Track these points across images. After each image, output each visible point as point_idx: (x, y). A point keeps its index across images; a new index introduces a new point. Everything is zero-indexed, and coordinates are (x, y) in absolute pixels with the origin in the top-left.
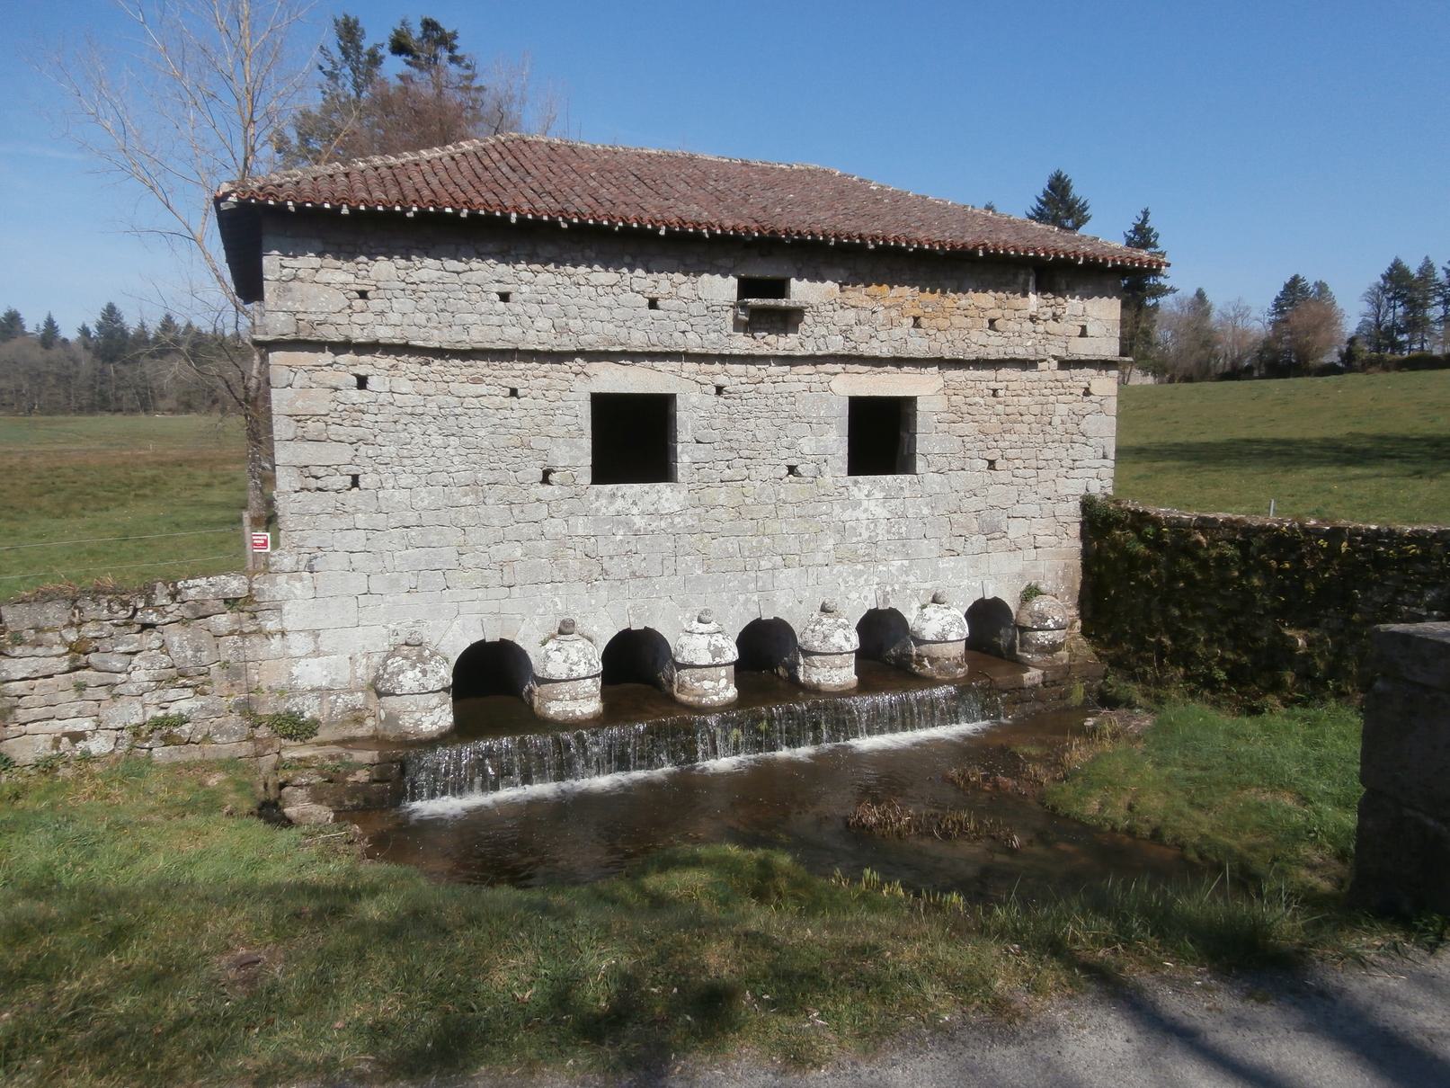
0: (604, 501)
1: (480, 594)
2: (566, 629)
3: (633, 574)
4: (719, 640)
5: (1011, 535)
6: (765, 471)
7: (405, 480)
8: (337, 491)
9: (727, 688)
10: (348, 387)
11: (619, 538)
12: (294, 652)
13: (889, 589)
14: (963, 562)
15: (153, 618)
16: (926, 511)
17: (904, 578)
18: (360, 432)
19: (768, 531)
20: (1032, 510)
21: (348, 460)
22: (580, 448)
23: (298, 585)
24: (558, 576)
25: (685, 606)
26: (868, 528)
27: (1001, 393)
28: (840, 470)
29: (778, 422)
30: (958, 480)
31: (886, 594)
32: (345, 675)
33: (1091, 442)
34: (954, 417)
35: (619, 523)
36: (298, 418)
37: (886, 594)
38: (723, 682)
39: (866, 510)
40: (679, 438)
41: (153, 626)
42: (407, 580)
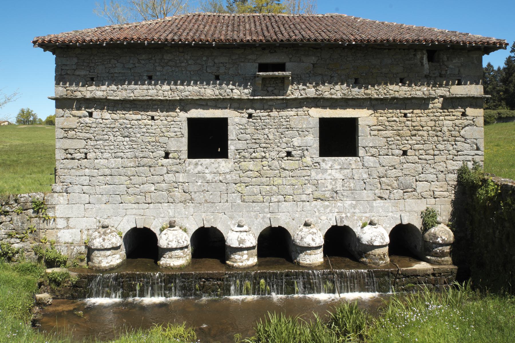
0: (192, 167)
1: (136, 206)
2: (172, 225)
3: (206, 201)
4: (243, 236)
5: (419, 191)
6: (274, 154)
7: (106, 155)
8: (79, 160)
9: (248, 260)
10: (85, 117)
11: (199, 184)
12: (58, 227)
13: (344, 215)
14: (387, 204)
15: (8, 209)
16: (365, 176)
17: (352, 210)
18: (88, 135)
19: (275, 183)
20: (432, 177)
21: (83, 147)
22: (182, 142)
23: (62, 198)
24: (171, 200)
25: (231, 218)
26: (331, 183)
27: (409, 115)
28: (315, 154)
30: (386, 160)
31: (341, 218)
32: (78, 238)
34: (380, 128)
35: (199, 177)
37: (341, 218)
38: (245, 257)
39: (330, 175)
40: (229, 138)
41: (8, 212)
42: (104, 198)
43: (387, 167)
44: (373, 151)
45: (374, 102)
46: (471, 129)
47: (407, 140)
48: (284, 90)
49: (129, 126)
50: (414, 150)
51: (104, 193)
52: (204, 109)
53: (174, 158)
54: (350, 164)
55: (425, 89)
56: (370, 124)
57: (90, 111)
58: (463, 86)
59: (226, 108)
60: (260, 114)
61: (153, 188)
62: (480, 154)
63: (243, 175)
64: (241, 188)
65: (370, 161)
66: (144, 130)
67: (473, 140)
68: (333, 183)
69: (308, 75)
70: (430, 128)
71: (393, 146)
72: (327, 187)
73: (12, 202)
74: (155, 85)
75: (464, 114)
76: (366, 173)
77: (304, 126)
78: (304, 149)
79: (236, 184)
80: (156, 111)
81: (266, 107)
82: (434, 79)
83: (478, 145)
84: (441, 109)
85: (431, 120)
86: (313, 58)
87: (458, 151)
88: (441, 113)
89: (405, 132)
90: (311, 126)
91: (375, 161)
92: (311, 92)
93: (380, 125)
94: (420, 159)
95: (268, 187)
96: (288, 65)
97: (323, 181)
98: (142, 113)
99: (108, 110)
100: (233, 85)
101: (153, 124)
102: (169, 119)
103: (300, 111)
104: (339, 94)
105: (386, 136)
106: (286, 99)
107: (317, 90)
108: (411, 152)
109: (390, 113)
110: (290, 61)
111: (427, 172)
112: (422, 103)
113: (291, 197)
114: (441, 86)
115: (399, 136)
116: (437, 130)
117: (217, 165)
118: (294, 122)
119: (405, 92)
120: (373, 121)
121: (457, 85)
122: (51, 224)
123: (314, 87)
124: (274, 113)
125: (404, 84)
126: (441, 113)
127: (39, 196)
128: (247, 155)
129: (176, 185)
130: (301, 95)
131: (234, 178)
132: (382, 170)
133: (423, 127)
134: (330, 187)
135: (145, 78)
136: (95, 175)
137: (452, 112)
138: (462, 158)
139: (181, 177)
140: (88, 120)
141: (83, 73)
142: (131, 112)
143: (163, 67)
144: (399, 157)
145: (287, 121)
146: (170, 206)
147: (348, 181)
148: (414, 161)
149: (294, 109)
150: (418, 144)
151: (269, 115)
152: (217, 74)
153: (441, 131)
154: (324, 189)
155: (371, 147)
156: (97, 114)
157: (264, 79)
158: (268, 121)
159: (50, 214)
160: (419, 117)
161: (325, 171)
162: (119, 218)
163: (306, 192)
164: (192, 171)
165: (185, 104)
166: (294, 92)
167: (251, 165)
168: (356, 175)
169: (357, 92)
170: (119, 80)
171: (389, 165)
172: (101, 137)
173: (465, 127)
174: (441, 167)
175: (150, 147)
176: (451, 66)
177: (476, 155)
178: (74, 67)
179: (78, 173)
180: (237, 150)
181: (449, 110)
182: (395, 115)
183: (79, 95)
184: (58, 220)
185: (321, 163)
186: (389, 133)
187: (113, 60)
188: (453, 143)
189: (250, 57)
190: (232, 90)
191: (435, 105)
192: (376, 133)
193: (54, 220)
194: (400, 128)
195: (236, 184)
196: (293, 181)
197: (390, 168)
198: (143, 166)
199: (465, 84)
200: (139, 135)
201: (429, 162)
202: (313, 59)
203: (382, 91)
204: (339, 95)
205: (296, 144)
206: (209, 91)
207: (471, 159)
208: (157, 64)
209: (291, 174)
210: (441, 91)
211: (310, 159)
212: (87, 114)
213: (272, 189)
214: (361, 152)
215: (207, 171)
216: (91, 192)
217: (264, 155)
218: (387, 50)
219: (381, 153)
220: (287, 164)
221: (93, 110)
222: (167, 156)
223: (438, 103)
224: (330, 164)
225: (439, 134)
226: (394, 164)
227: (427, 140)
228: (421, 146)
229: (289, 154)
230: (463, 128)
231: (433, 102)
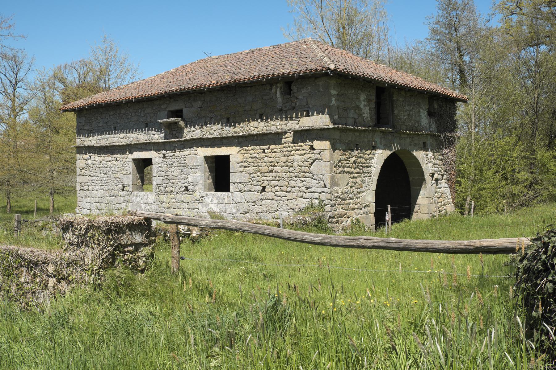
0: (135, 197)
7: (97, 188)
10: (89, 159)
16: (234, 211)
18: (89, 173)
28: (201, 189)
29: (182, 168)
33: (315, 177)
34: (246, 164)
45: (240, 140)
46: (318, 164)
47: (266, 177)
49: (106, 166)
54: (224, 199)
55: (278, 124)
56: (238, 161)
59: (151, 150)
60: (169, 154)
62: (326, 191)
63: (160, 205)
66: (113, 169)
70: (283, 164)
74: (118, 133)
75: (312, 148)
76: (234, 208)
78: (195, 184)
81: (172, 148)
82: (285, 113)
84: (293, 142)
85: (284, 156)
87: (307, 188)
89: (264, 169)
90: (198, 164)
93: (245, 162)
94: (276, 195)
96: (185, 111)
98: (112, 156)
100: (155, 131)
105: (249, 172)
108: (268, 188)
110: (186, 107)
111: (281, 209)
114: (291, 119)
116: (289, 165)
117: (146, 197)
119: (262, 128)
120: (240, 158)
121: (306, 116)
123: (200, 128)
124: (177, 154)
128: (163, 189)
133: (278, 163)
135: (113, 129)
137: (302, 146)
138: (310, 195)
140: (89, 162)
141: (87, 127)
149: (189, 149)
150: (274, 180)
153: (292, 167)
156: (93, 156)
158: (173, 160)
160: (275, 152)
167: (164, 198)
168: (228, 210)
169: (228, 131)
170: (101, 132)
172: (94, 174)
176: (300, 97)
177: (323, 192)
178: (84, 124)
181: (300, 144)
183: (86, 144)
186: (251, 169)
188: (303, 179)
189: (162, 107)
190: (154, 135)
194: (260, 164)
197: (253, 204)
198: (113, 196)
199: (312, 115)
202: (199, 103)
204: (216, 135)
210: (293, 125)
214: (232, 187)
215: (142, 202)
217: (171, 189)
218: (249, 88)
219: (246, 189)
220: (186, 197)
221: (91, 154)
222: (123, 190)
223: (289, 137)
224: (211, 198)
225: (291, 169)
226: (255, 200)
227: (280, 176)
229: (187, 189)
230: (312, 163)
231: (285, 136)
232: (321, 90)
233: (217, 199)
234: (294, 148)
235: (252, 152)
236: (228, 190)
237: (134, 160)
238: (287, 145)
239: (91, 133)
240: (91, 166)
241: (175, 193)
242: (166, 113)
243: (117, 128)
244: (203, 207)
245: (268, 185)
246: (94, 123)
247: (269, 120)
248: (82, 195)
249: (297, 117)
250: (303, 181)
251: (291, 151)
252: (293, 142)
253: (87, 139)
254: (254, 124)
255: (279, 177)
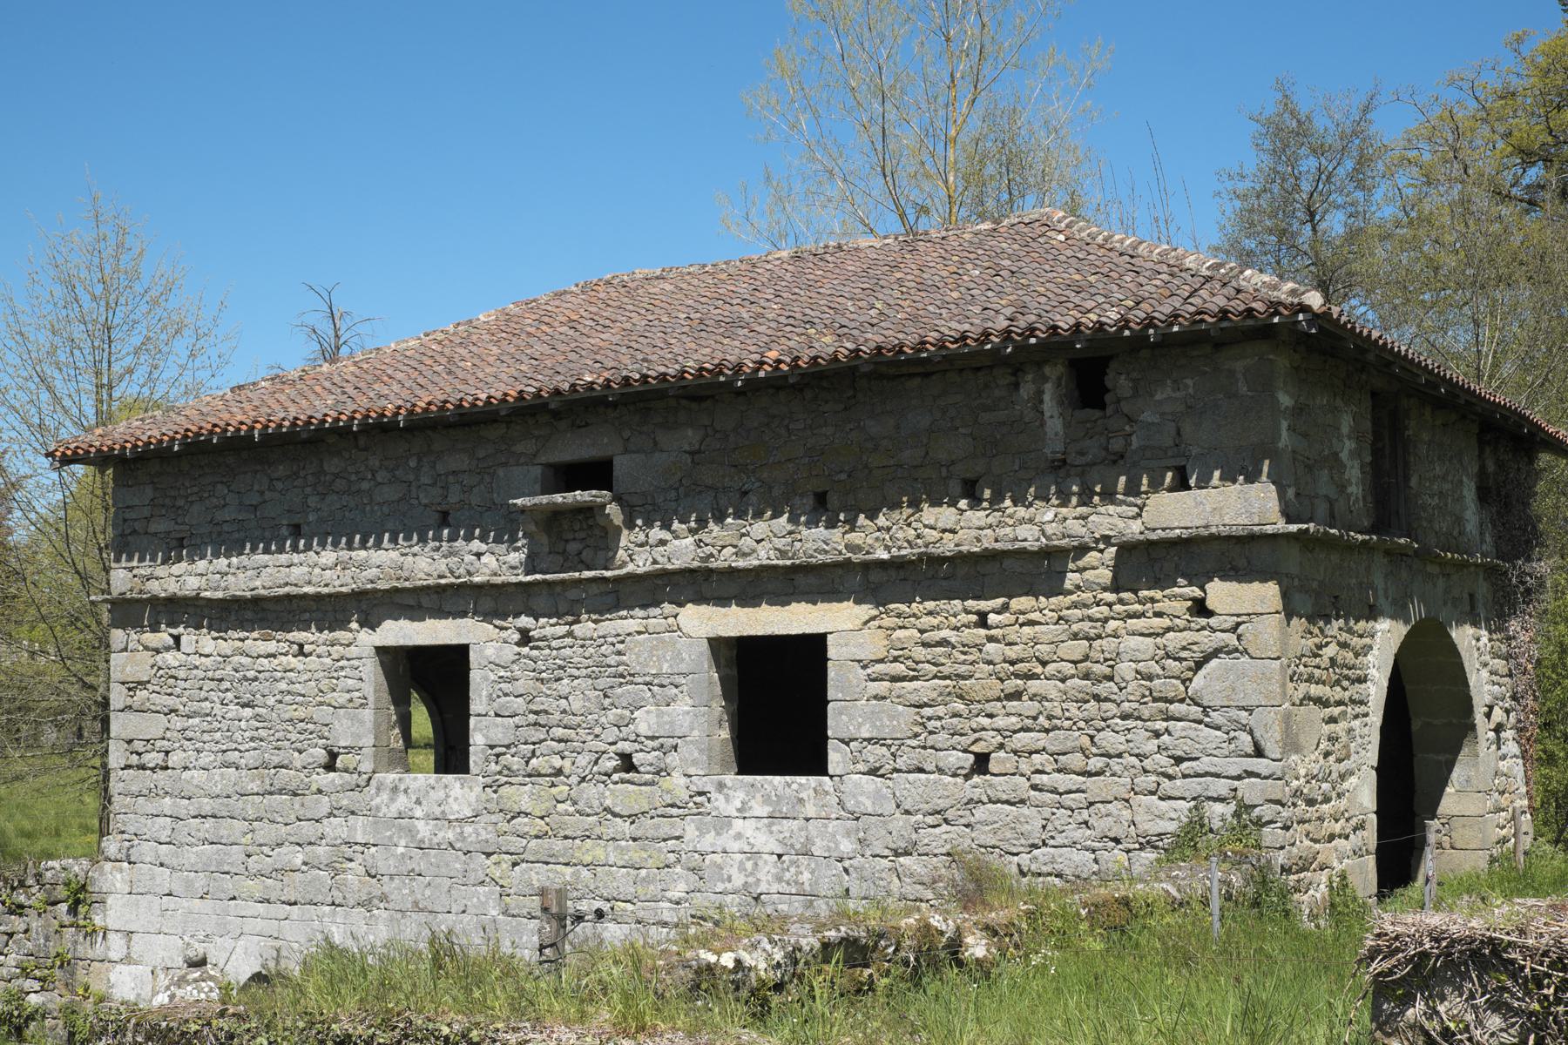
0: (385, 796)
6: (583, 760)
7: (206, 759)
8: (152, 769)
10: (168, 649)
11: (401, 850)
12: (114, 955)
15: (22, 899)
18: (171, 702)
21: (160, 734)
22: (362, 722)
23: (119, 876)
26: (742, 868)
28: (695, 763)
29: (603, 682)
30: (911, 787)
33: (1216, 717)
34: (899, 668)
35: (401, 828)
36: (134, 686)
41: (21, 906)
42: (200, 882)
43: (920, 817)
44: (876, 753)
45: (875, 576)
46: (1228, 670)
47: (991, 716)
48: (608, 549)
49: (251, 674)
50: (1015, 752)
51: (199, 867)
52: (412, 619)
53: (346, 771)
54: (801, 800)
55: (1049, 516)
56: (866, 655)
57: (174, 631)
58: (1195, 492)
59: (463, 615)
60: (549, 631)
61: (298, 860)
62: (1265, 772)
63: (504, 826)
64: (499, 868)
65: (863, 791)
66: (283, 686)
67: (1234, 713)
68: (749, 865)
69: (673, 494)
70: (1068, 668)
71: (941, 739)
72: (729, 879)
73: (30, 882)
74: (308, 548)
75: (1200, 608)
76: (848, 834)
77: (665, 668)
78: (666, 745)
79: (488, 855)
80: (307, 629)
81: (561, 609)
82: (1079, 474)
83: (1257, 734)
84: (1116, 587)
85: (1075, 636)
86: (690, 432)
87: (1179, 760)
88: (1110, 605)
89: (983, 684)
90: (683, 668)
91: (878, 791)
92: (679, 548)
93: (896, 659)
94: (1034, 787)
95: (569, 870)
96: (622, 465)
97: (717, 858)
98: (280, 635)
99: (210, 628)
100: (483, 539)
101: (301, 667)
102: (337, 651)
103: (656, 617)
104: (763, 554)
105: (914, 699)
106: (604, 579)
107: (699, 543)
108: (1003, 761)
109: (930, 613)
110: (626, 451)
111: (1059, 840)
112: (1040, 570)
113: (629, 907)
114: (1109, 496)
115: (961, 697)
116: (1096, 676)
117: (442, 794)
118: (638, 656)
119: (974, 533)
120: (873, 644)
121: (1170, 490)
122: (99, 950)
123: (693, 532)
124: (585, 628)
125: (975, 502)
126: (1110, 605)
127: (78, 867)
128: (516, 763)
129: (349, 852)
130: (655, 562)
131: (484, 835)
132: (900, 821)
133: (1044, 664)
134: (738, 881)
135: (284, 531)
136: (183, 813)
137: (1153, 600)
139: (360, 829)
140: (171, 658)
141: (158, 526)
142: (255, 634)
143: (323, 496)
144: (960, 780)
145: (619, 653)
146: (334, 913)
147: (792, 863)
148: (1012, 797)
149: (638, 612)
151: (570, 634)
152: (444, 507)
153: (1110, 678)
154: (720, 887)
155: (869, 740)
156: (189, 638)
157: (554, 517)
158: (567, 652)
159: (98, 920)
160: (1029, 624)
161: (724, 822)
162: (228, 942)
163: (669, 894)
164: (384, 809)
165: (369, 605)
166: (644, 550)
167: (522, 796)
169: (821, 542)
170: (230, 541)
171: (926, 807)
172: (195, 706)
173: (1207, 658)
174: (1114, 819)
175: (293, 737)
176: (1147, 416)
178: (146, 512)
179: (151, 808)
180: (492, 747)
181: (1143, 593)
182: (948, 617)
183: (154, 587)
184: (111, 936)
185: (713, 796)
186: (923, 689)
187: (219, 486)
188: (1160, 725)
189: (519, 448)
190: (479, 555)
191: (1089, 575)
192: (882, 687)
193: (104, 937)
194: (963, 669)
195: (488, 855)
196: (635, 853)
197: (930, 820)
198: (280, 792)
199: (1203, 484)
200: (271, 701)
201: (1068, 800)
203: (900, 535)
204: (764, 556)
205: (643, 729)
206: (423, 563)
207: (1224, 792)
208: (308, 490)
209: (625, 827)
210: (1116, 520)
211: (684, 780)
212: (171, 641)
213: (576, 875)
214: (836, 757)
215: (418, 813)
216: (175, 862)
217: (557, 762)
218: (916, 381)
219: (900, 763)
220: (623, 795)
221: (181, 629)
222: (330, 767)
223: (1099, 567)
224: (738, 797)
225: (1105, 688)
226: (942, 804)
227: (1058, 712)
228: (1039, 740)
229: (627, 763)
230: (1199, 665)
231: (1080, 563)
232: (1243, 389)
233: (767, 800)
234: (1118, 608)
235: (927, 621)
236: (818, 766)
237: (381, 651)
238: (1087, 596)
239: (179, 546)
240: (182, 674)
241: (574, 779)
242: (537, 471)
243: (305, 529)
244: (702, 834)
245: (1001, 746)
246: (196, 508)
247: (1008, 502)
248: (134, 789)
249: (1133, 490)
250: (1157, 735)
251: (1106, 620)
252: (1116, 587)
253: (161, 571)
254: (944, 515)
255: (1050, 718)
